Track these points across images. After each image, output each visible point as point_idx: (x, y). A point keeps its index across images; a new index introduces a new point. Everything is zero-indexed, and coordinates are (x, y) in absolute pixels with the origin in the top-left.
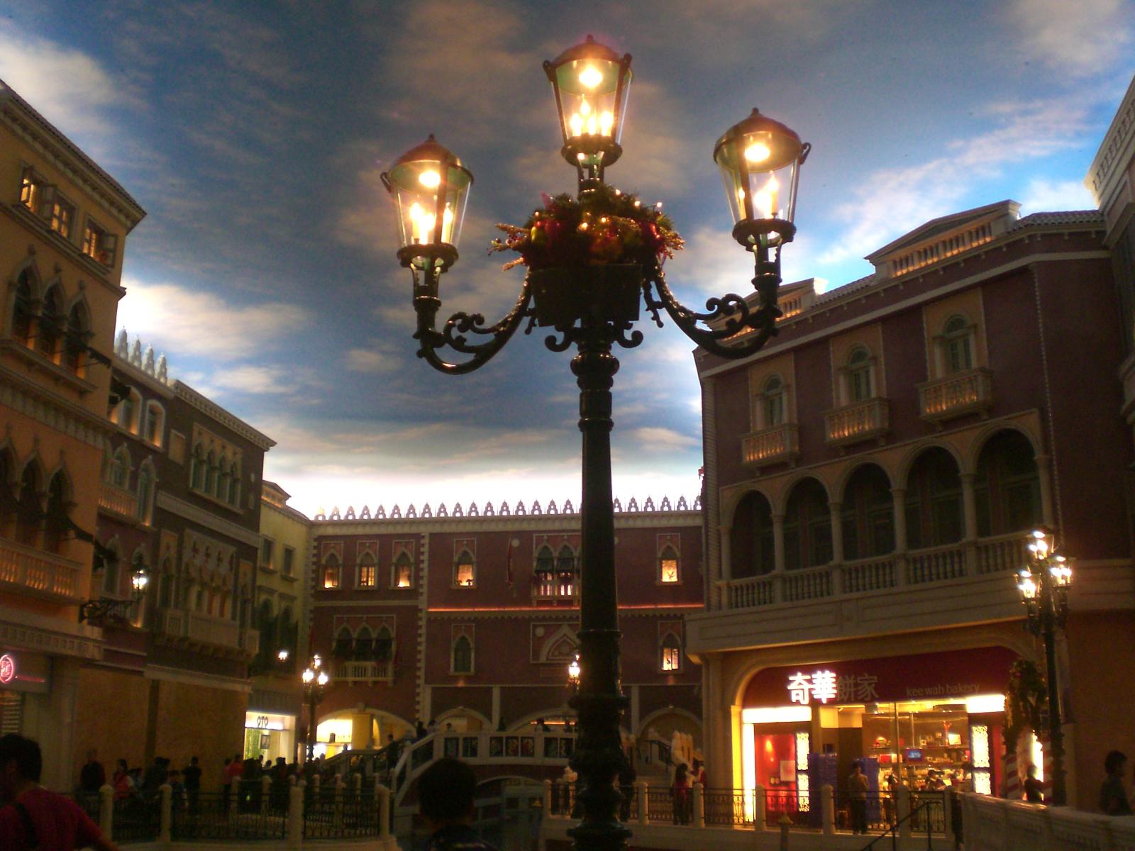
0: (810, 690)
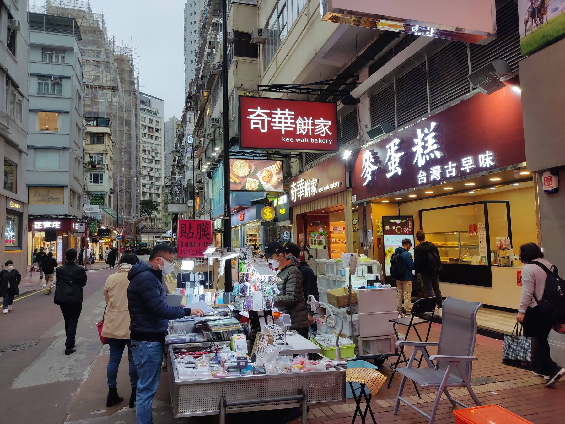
0: (269, 122)
